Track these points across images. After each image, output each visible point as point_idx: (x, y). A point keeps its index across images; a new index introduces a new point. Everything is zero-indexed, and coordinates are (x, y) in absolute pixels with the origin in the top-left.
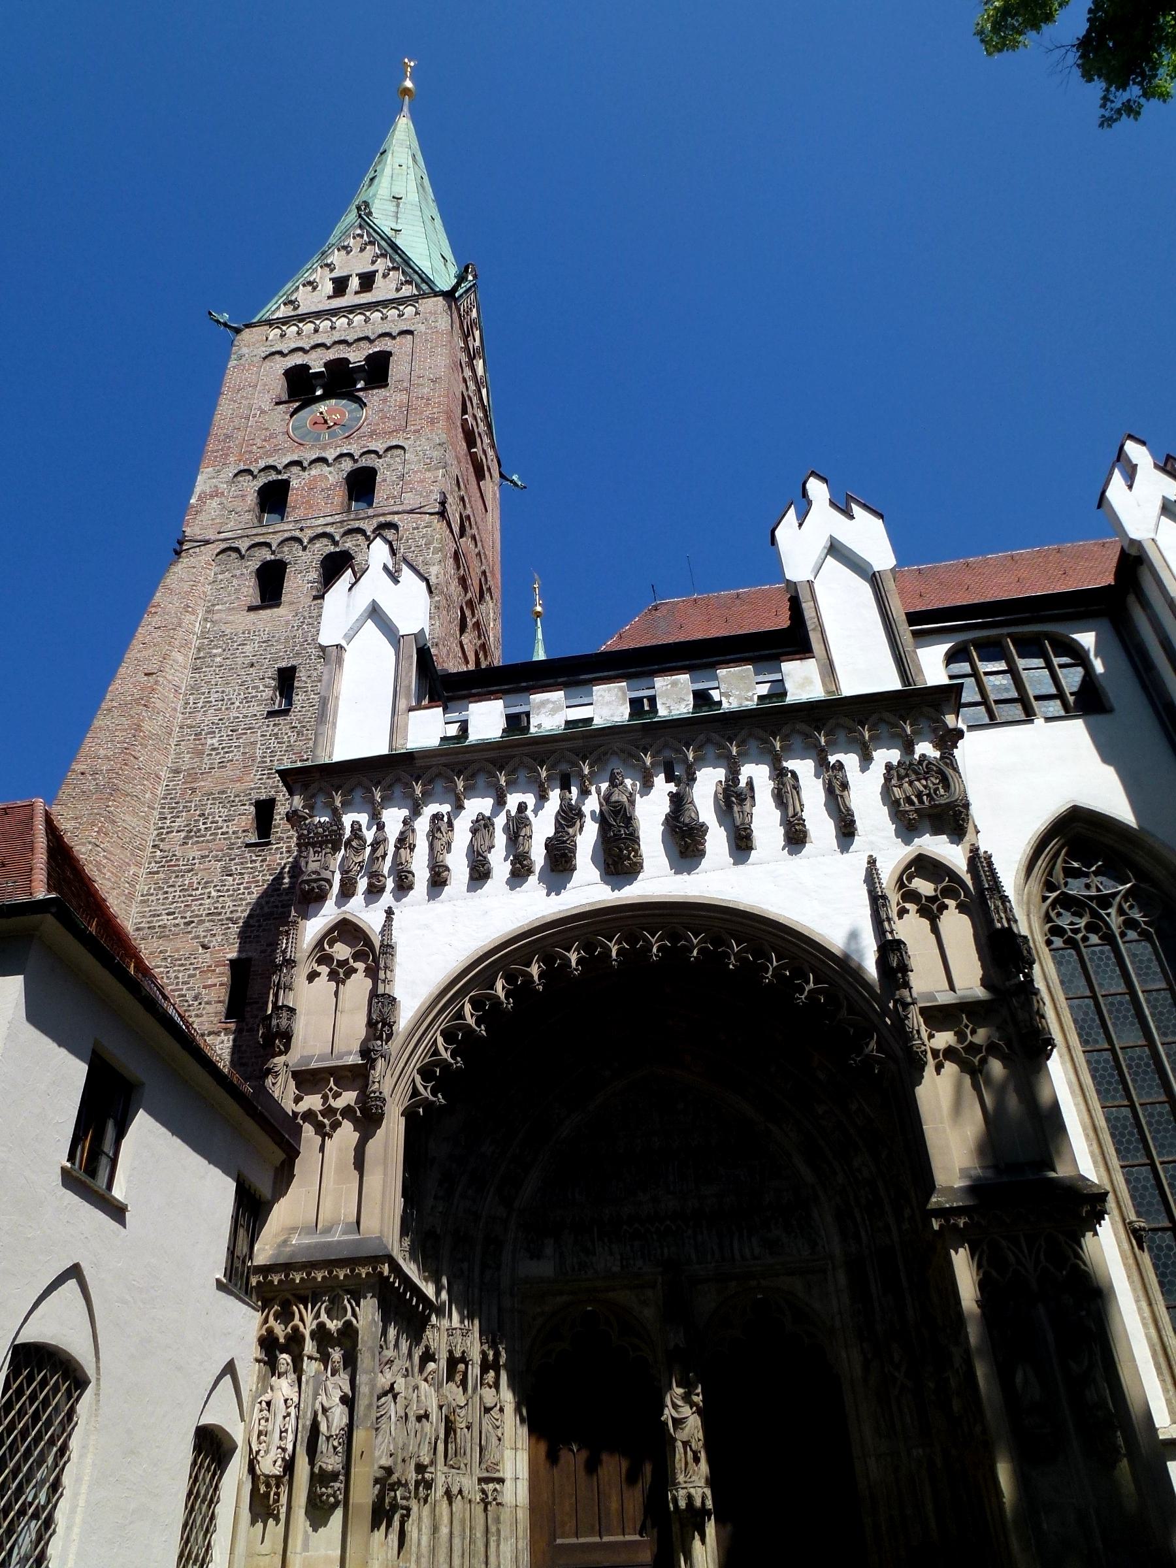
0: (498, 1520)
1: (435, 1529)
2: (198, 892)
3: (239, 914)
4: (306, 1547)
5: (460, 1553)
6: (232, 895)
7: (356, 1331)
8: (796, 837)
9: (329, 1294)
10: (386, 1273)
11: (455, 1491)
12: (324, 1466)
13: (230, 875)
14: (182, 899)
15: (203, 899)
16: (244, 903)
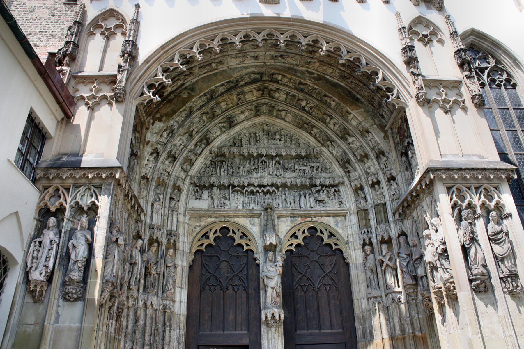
0: (170, 320)
1: (136, 321)
2: (35, 22)
3: (56, 33)
5: (149, 334)
6: (54, 24)
7: (97, 208)
9: (82, 187)
11: (149, 304)
12: (71, 276)
13: (54, 16)
14: (27, 23)
15: (38, 25)
16: (60, 28)
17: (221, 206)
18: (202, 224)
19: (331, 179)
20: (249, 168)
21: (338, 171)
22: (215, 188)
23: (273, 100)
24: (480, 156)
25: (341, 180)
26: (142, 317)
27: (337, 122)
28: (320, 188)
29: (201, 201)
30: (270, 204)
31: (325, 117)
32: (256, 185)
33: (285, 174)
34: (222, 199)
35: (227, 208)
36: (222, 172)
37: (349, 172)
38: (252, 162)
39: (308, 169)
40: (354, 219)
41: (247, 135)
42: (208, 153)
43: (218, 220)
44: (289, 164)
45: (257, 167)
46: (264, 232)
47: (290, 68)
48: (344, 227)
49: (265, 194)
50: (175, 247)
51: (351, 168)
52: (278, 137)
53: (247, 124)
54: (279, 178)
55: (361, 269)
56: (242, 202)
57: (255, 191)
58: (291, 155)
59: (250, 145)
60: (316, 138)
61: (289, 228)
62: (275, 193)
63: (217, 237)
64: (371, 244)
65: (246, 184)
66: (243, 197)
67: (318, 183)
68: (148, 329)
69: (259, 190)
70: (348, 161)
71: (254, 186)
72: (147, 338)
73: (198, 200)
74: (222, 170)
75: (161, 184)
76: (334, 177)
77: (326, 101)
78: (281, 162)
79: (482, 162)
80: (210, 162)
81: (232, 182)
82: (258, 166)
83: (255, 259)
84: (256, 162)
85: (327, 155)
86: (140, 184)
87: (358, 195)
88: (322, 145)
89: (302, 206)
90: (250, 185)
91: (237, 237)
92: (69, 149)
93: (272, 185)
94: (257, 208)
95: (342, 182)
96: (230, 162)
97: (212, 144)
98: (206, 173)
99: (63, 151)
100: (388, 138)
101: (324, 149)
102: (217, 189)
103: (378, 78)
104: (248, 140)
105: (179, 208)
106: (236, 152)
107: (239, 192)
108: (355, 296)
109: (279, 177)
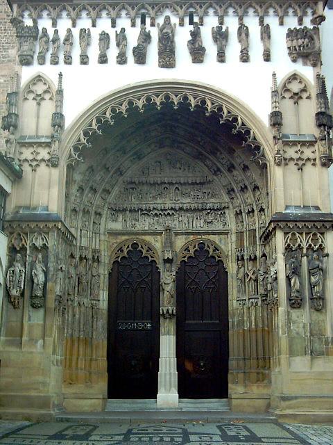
0: (97, 314)
1: (74, 315)
4: (29, 320)
8: (245, 57)
18: (118, 241)
24: (317, 208)
26: (78, 312)
28: (209, 211)
35: (136, 228)
37: (233, 198)
40: (234, 238)
42: (122, 182)
43: (131, 237)
46: (164, 247)
48: (226, 244)
50: (98, 261)
52: (178, 165)
55: (234, 277)
56: (147, 223)
61: (183, 244)
63: (130, 251)
64: (243, 259)
68: (82, 321)
70: (233, 190)
72: (82, 327)
75: (85, 212)
79: (315, 215)
83: (158, 268)
86: (71, 215)
89: (194, 227)
90: (154, 209)
91: (144, 251)
92: (24, 202)
93: (172, 209)
94: (159, 228)
99: (18, 205)
100: (263, 175)
101: (215, 177)
103: (249, 138)
108: (230, 297)
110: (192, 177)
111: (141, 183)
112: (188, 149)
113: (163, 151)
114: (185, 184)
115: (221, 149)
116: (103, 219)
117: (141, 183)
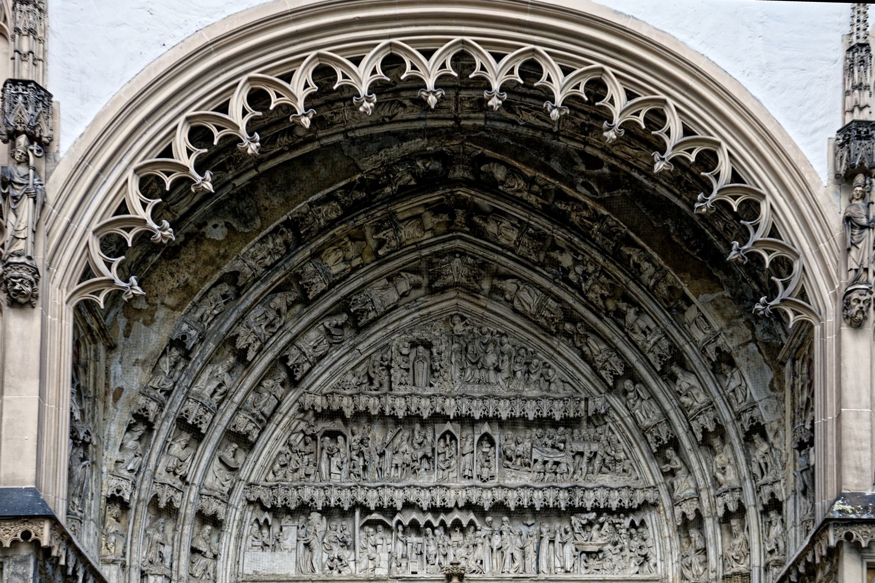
10: (45, 543)
17: (331, 569)
19: (624, 493)
20: (407, 457)
21: (647, 469)
22: (315, 517)
23: (480, 245)
25: (650, 496)
27: (653, 326)
28: (593, 516)
29: (278, 554)
30: (458, 564)
31: (623, 306)
32: (425, 509)
33: (504, 476)
34: (334, 546)
35: (346, 572)
36: (334, 469)
37: (672, 473)
38: (418, 438)
39: (565, 459)
41: (405, 351)
44: (517, 443)
45: (430, 455)
47: (532, 143)
49: (447, 531)
51: (679, 464)
53: (405, 317)
54: (490, 489)
57: (422, 523)
58: (524, 418)
59: (414, 385)
60: (594, 369)
62: (476, 530)
65: (399, 505)
66: (389, 541)
67: (589, 505)
69: (432, 520)
71: (421, 510)
73: (269, 550)
74: (335, 461)
76: (633, 486)
77: (630, 256)
78: (496, 438)
80: (301, 435)
81: (360, 499)
82: (433, 450)
84: (430, 438)
85: (622, 419)
87: (690, 542)
88: (610, 390)
90: (408, 505)
93: (469, 506)
95: (652, 501)
96: (358, 437)
97: (308, 381)
98: (289, 469)
102: (322, 518)
104: (407, 370)
105: (219, 575)
106: (374, 408)
107: (380, 527)
109: (488, 484)
110: (536, 400)
111: (362, 416)
112: (529, 299)
113: (446, 303)
114: (513, 422)
115: (643, 297)
116: (227, 542)
117: (362, 416)
